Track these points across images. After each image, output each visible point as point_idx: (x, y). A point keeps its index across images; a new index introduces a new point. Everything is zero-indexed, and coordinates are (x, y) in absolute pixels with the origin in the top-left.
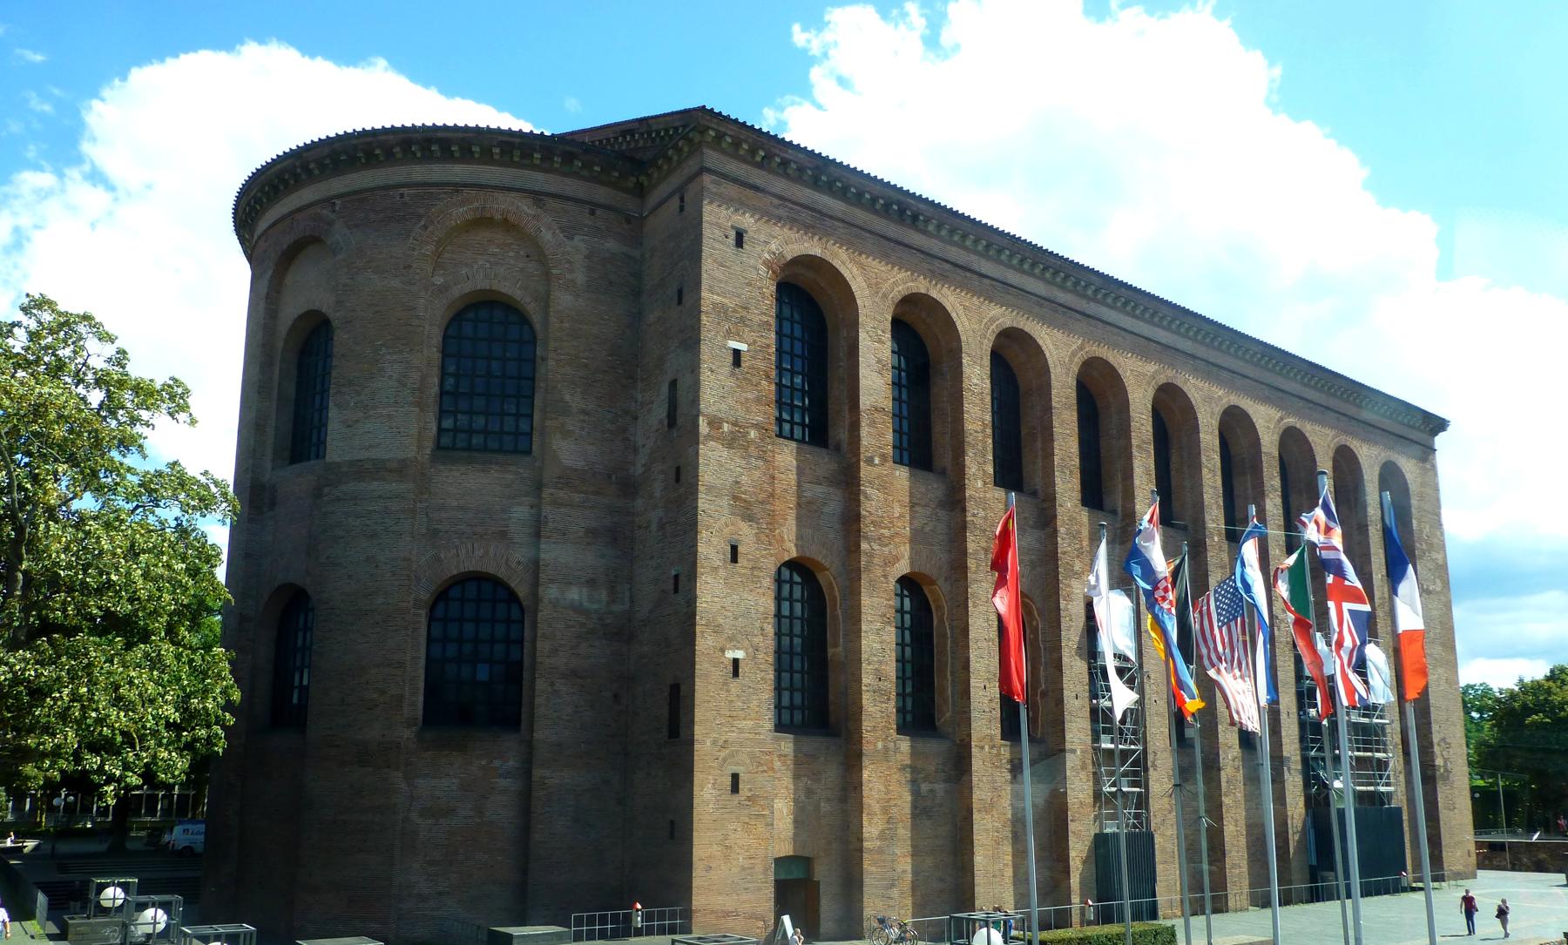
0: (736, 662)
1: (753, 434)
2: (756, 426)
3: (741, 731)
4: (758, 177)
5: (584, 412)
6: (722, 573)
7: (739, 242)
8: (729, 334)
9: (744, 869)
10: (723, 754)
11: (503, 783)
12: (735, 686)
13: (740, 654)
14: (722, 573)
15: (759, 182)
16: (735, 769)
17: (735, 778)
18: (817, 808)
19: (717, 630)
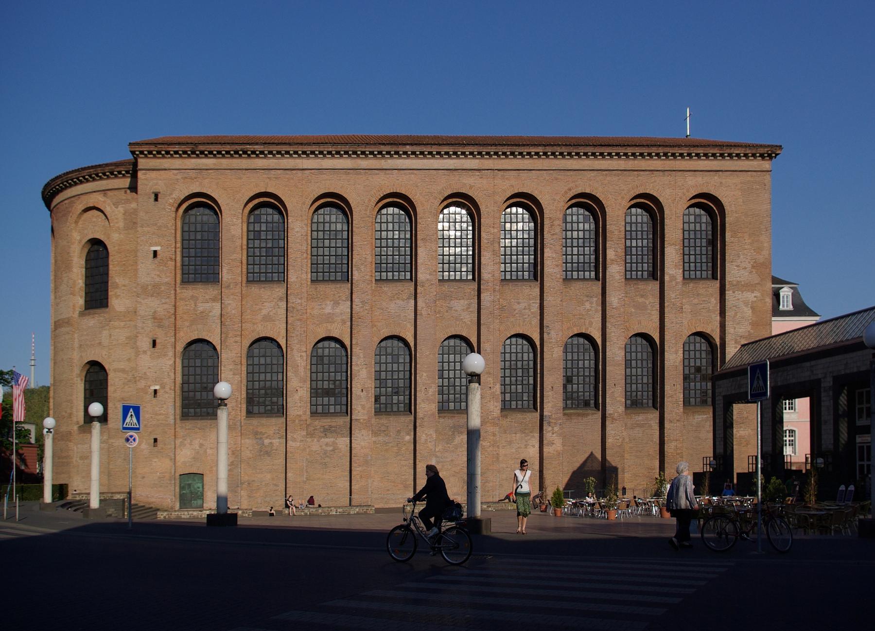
5: (124, 286)
6: (149, 353)
13: (157, 387)
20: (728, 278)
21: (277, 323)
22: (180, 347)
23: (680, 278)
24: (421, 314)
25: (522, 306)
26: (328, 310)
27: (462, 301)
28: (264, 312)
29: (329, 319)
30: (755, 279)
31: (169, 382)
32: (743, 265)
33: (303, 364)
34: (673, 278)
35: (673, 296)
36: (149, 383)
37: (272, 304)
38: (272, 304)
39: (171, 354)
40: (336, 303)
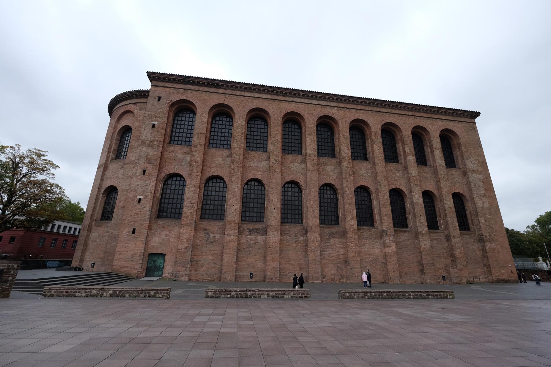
0: (140, 200)
1: (155, 143)
2: (158, 141)
3: (138, 217)
4: (167, 85)
6: (140, 177)
7: (159, 99)
8: (152, 121)
9: (132, 255)
10: (131, 223)
11: (106, 234)
12: (138, 206)
13: (141, 197)
14: (140, 177)
15: (168, 86)
16: (134, 227)
17: (134, 231)
18: (169, 240)
19: (135, 191)
20: (468, 167)
21: (224, 168)
22: (162, 176)
23: (444, 165)
24: (309, 170)
25: (363, 172)
26: (255, 164)
27: (330, 167)
28: (217, 162)
29: (256, 169)
30: (481, 169)
31: (150, 195)
32: (473, 162)
33: (239, 191)
34: (440, 165)
35: (442, 173)
36: (136, 194)
37: (222, 159)
38: (222, 159)
39: (154, 179)
40: (260, 161)
